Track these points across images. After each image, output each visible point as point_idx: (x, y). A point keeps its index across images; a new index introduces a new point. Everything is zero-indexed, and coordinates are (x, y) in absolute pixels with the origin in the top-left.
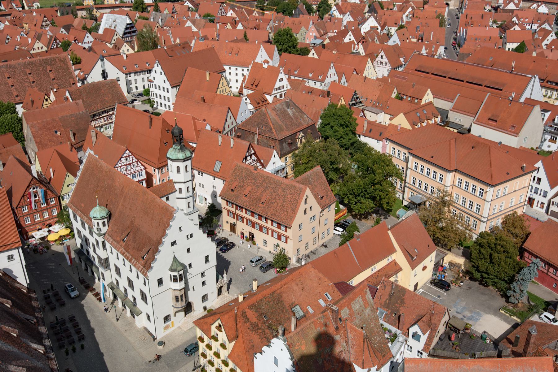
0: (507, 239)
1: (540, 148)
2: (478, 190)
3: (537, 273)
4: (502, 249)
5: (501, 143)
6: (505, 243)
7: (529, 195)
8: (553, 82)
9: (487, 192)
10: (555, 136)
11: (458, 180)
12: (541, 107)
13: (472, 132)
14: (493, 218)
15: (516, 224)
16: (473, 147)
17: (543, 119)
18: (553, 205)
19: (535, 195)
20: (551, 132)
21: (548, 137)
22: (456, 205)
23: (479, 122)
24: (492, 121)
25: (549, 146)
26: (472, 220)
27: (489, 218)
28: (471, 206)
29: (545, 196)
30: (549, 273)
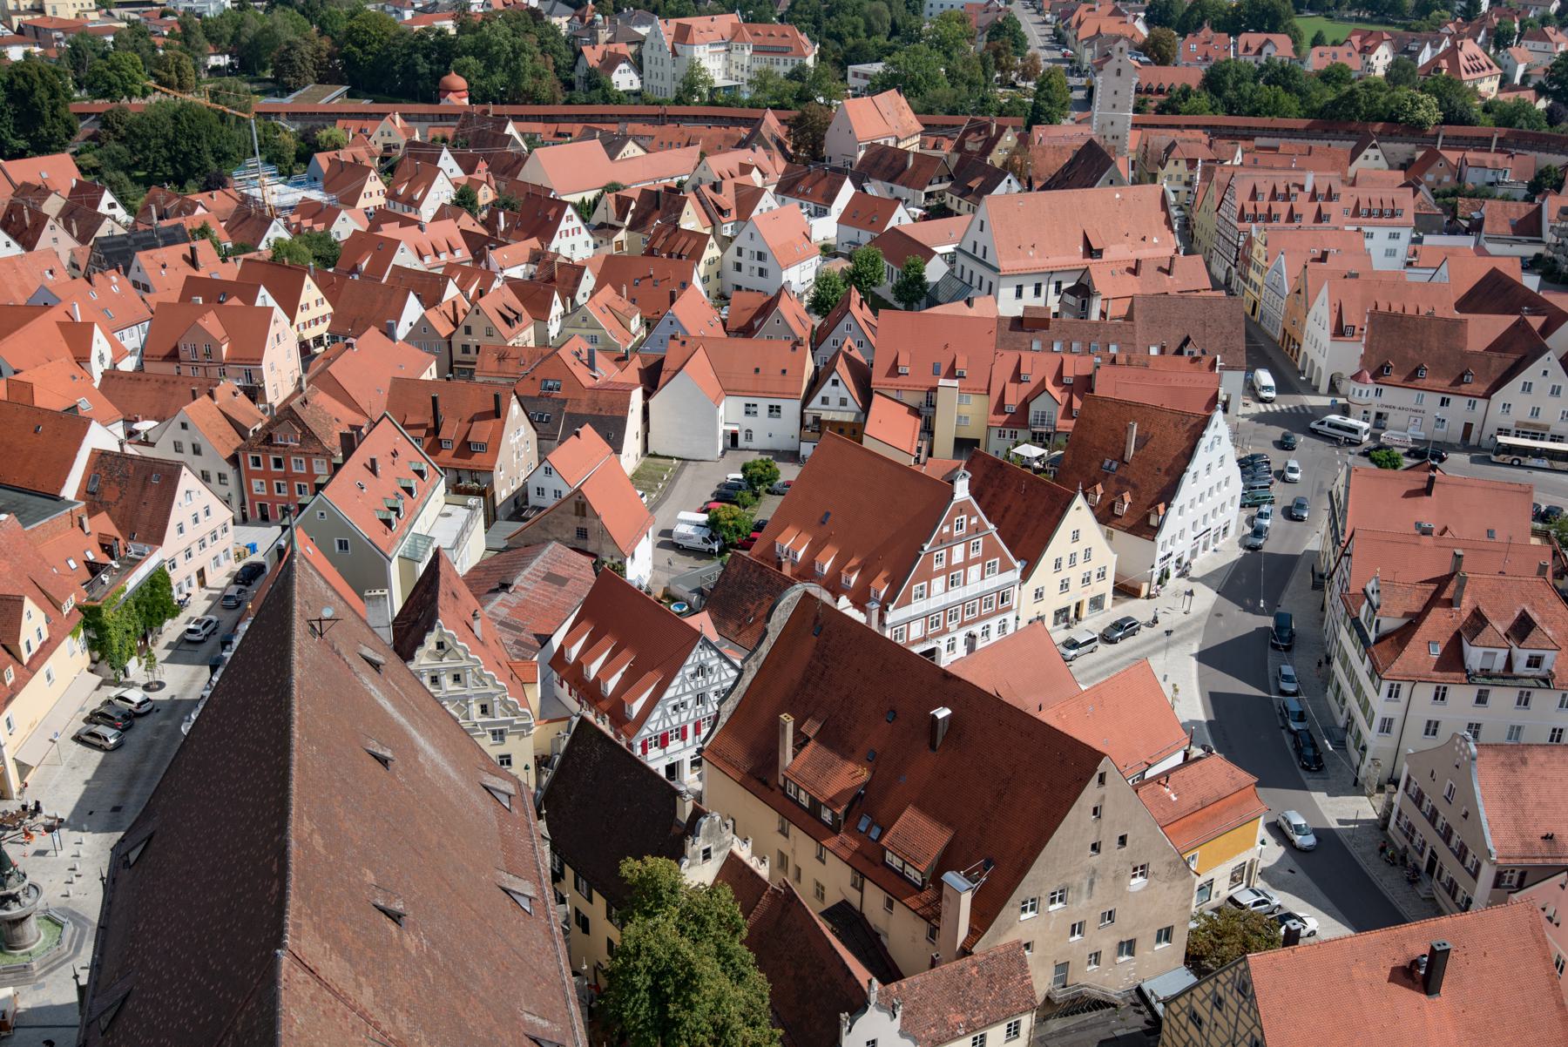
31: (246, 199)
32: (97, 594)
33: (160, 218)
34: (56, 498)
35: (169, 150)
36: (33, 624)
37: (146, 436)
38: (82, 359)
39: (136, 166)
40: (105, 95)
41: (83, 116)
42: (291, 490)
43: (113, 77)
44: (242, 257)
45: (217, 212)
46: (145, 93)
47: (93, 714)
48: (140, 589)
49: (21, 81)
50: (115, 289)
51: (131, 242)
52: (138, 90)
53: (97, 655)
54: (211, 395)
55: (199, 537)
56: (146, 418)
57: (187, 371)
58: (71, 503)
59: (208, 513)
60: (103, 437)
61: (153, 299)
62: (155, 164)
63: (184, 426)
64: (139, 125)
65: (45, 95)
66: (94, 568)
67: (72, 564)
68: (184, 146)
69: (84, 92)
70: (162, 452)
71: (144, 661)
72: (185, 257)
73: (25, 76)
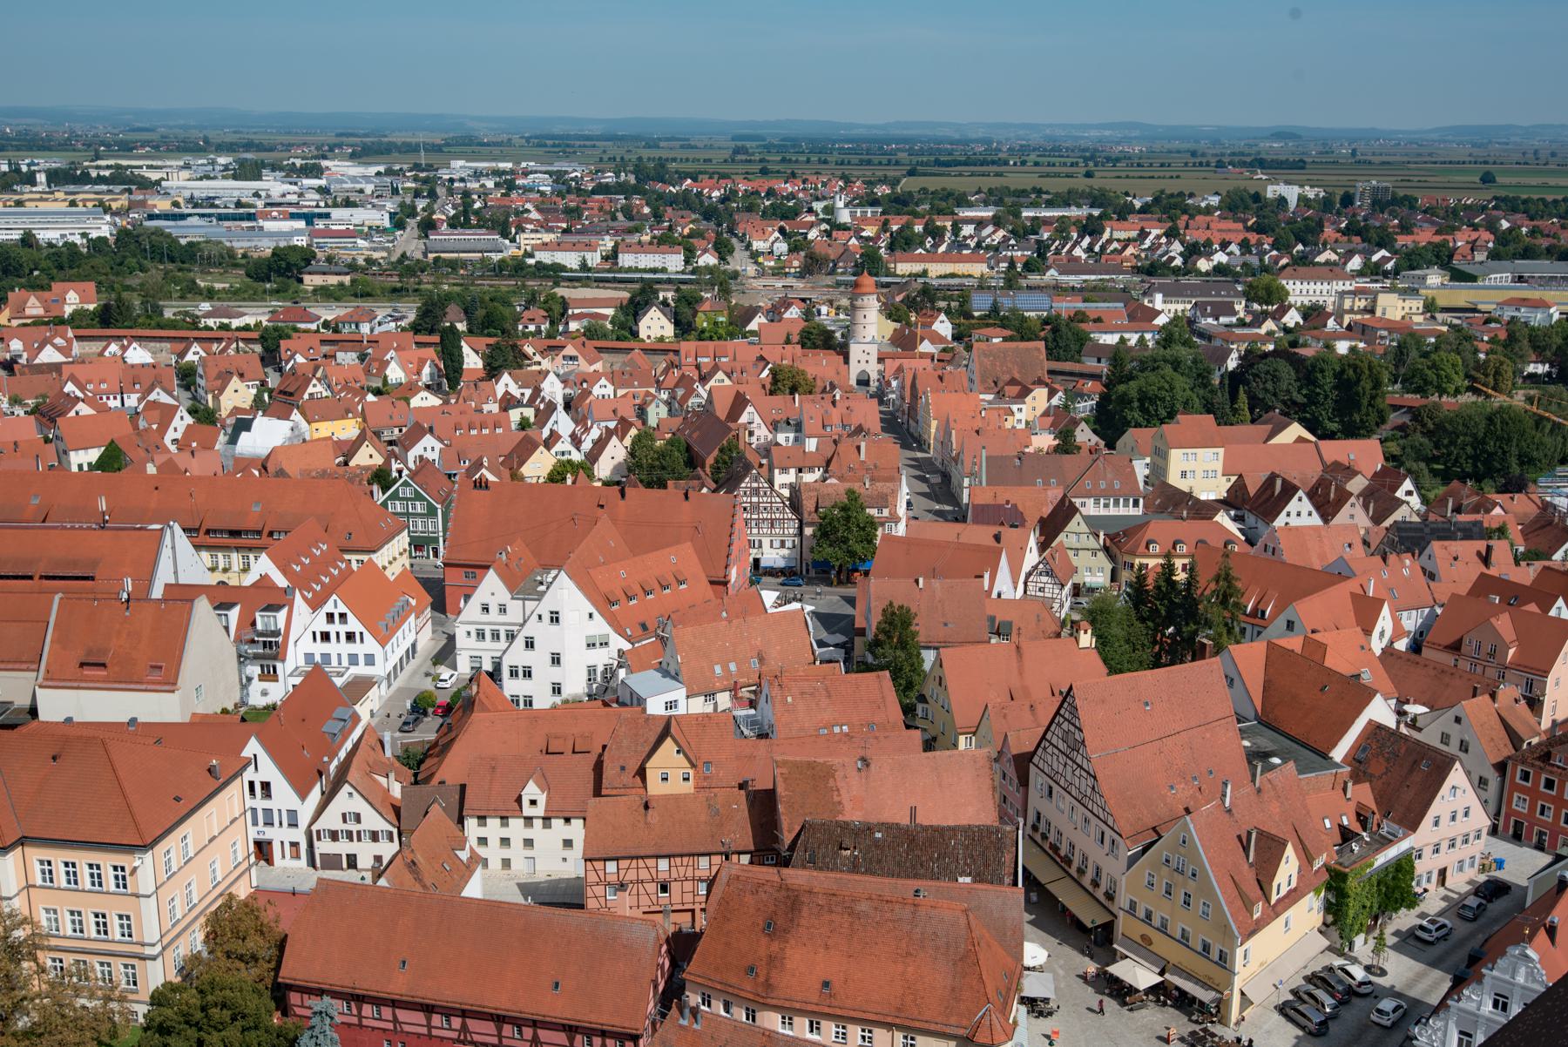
0: (230, 979)
1: (243, 703)
2: (109, 876)
3: (336, 1036)
4: (227, 1014)
5: (133, 720)
6: (228, 992)
7: (253, 834)
8: (221, 532)
9: (134, 870)
10: (271, 663)
11: (38, 867)
12: (211, 602)
13: (44, 715)
14: (178, 936)
15: (242, 927)
16: (54, 758)
17: (227, 628)
18: (319, 839)
19: (268, 830)
20: (256, 657)
21: (254, 670)
22: (53, 942)
23: (54, 680)
24: (93, 668)
25: (264, 693)
26: (118, 966)
27: (165, 941)
28: (102, 928)
29: (293, 824)
30: (365, 1022)
31: (1546, 507)
32: (1346, 859)
33: (1458, 510)
34: (1325, 756)
36: (1288, 870)
37: (1414, 720)
38: (1368, 632)
39: (1435, 459)
40: (1415, 391)
41: (1396, 408)
42: (1557, 816)
43: (1430, 374)
44: (1538, 565)
45: (1516, 515)
46: (1457, 392)
47: (1313, 974)
48: (1385, 868)
49: (1351, 372)
50: (1406, 572)
51: (1427, 530)
52: (1451, 388)
53: (1330, 919)
54: (1493, 696)
55: (1451, 836)
56: (1415, 702)
57: (1464, 665)
58: (1337, 765)
59: (1466, 814)
60: (1380, 711)
61: (1443, 590)
62: (1456, 460)
63: (1458, 720)
64: (1451, 421)
66: (1346, 835)
67: (1327, 822)
68: (1491, 446)
69: (1398, 386)
70: (1430, 737)
71: (1372, 943)
72: (1479, 553)
73: (1355, 367)
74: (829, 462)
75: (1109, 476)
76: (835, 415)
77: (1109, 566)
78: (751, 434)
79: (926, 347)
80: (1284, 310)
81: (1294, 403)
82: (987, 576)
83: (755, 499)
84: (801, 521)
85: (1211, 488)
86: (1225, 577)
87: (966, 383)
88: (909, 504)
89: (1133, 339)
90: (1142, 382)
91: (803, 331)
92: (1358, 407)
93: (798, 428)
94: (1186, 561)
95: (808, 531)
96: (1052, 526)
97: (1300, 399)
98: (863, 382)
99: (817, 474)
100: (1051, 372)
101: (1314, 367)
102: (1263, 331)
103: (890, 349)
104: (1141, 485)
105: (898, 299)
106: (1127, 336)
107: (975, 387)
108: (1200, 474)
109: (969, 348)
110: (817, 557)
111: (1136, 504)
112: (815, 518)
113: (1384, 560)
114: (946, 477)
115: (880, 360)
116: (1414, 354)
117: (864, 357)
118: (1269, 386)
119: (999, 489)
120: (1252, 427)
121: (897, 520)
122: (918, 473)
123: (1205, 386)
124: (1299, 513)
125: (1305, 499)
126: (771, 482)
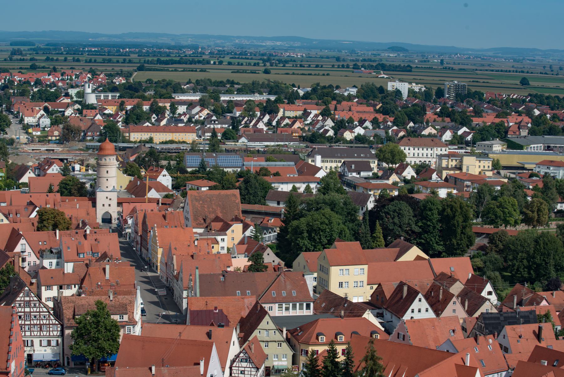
33: (520, 303)
35: (528, 261)
39: (505, 269)
40: (492, 222)
41: (479, 234)
43: (499, 211)
46: (516, 223)
49: (449, 210)
50: (490, 348)
51: (502, 318)
52: (512, 221)
61: (513, 359)
62: (518, 270)
65: (461, 220)
68: (538, 260)
69: (480, 220)
72: (534, 332)
73: (452, 208)
74: (82, 281)
75: (289, 287)
76: (87, 244)
77: (290, 353)
78: (24, 260)
79: (153, 194)
80: (403, 167)
81: (413, 232)
82: (202, 363)
83: (27, 310)
84: (62, 326)
85: (360, 294)
86: (371, 358)
87: (183, 221)
88: (143, 311)
89: (302, 187)
90: (309, 218)
91: (62, 183)
92: (454, 233)
93: (59, 255)
94: (344, 347)
95: (68, 332)
96: (249, 324)
97: (417, 229)
98: (107, 220)
99: (74, 290)
100: (245, 212)
101: (425, 206)
102: (390, 182)
103: (126, 196)
104: (311, 293)
105: (132, 159)
106: (297, 185)
107: (190, 223)
108: (352, 284)
109: (184, 195)
110: (75, 353)
111: (308, 307)
112: (73, 322)
113: (476, 340)
114: (170, 290)
115: (119, 204)
116: (488, 198)
117: (107, 202)
118: (396, 220)
119: (209, 299)
120: (386, 249)
121: (134, 323)
122: (149, 287)
123: (353, 221)
124: (420, 310)
125: (423, 300)
126: (39, 296)
